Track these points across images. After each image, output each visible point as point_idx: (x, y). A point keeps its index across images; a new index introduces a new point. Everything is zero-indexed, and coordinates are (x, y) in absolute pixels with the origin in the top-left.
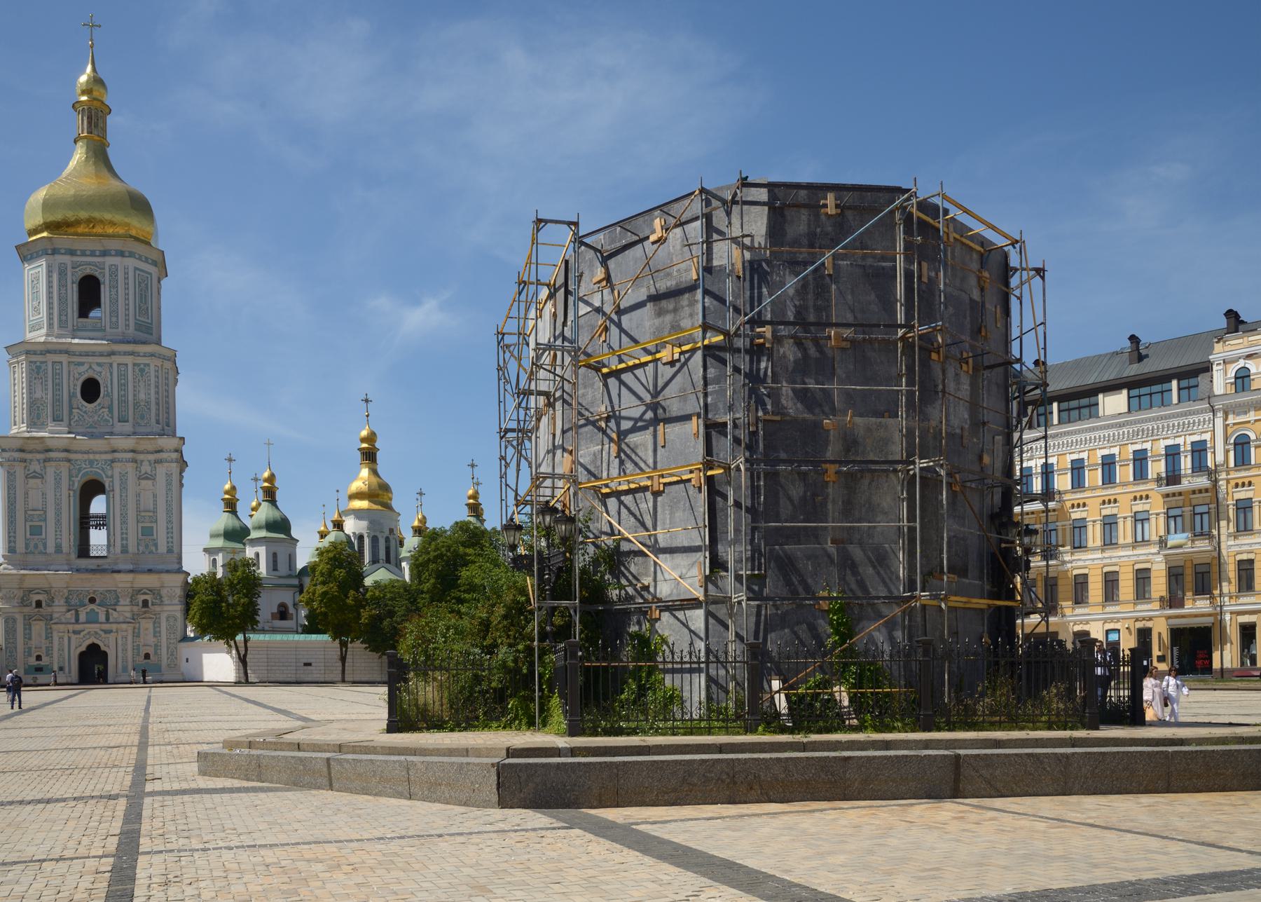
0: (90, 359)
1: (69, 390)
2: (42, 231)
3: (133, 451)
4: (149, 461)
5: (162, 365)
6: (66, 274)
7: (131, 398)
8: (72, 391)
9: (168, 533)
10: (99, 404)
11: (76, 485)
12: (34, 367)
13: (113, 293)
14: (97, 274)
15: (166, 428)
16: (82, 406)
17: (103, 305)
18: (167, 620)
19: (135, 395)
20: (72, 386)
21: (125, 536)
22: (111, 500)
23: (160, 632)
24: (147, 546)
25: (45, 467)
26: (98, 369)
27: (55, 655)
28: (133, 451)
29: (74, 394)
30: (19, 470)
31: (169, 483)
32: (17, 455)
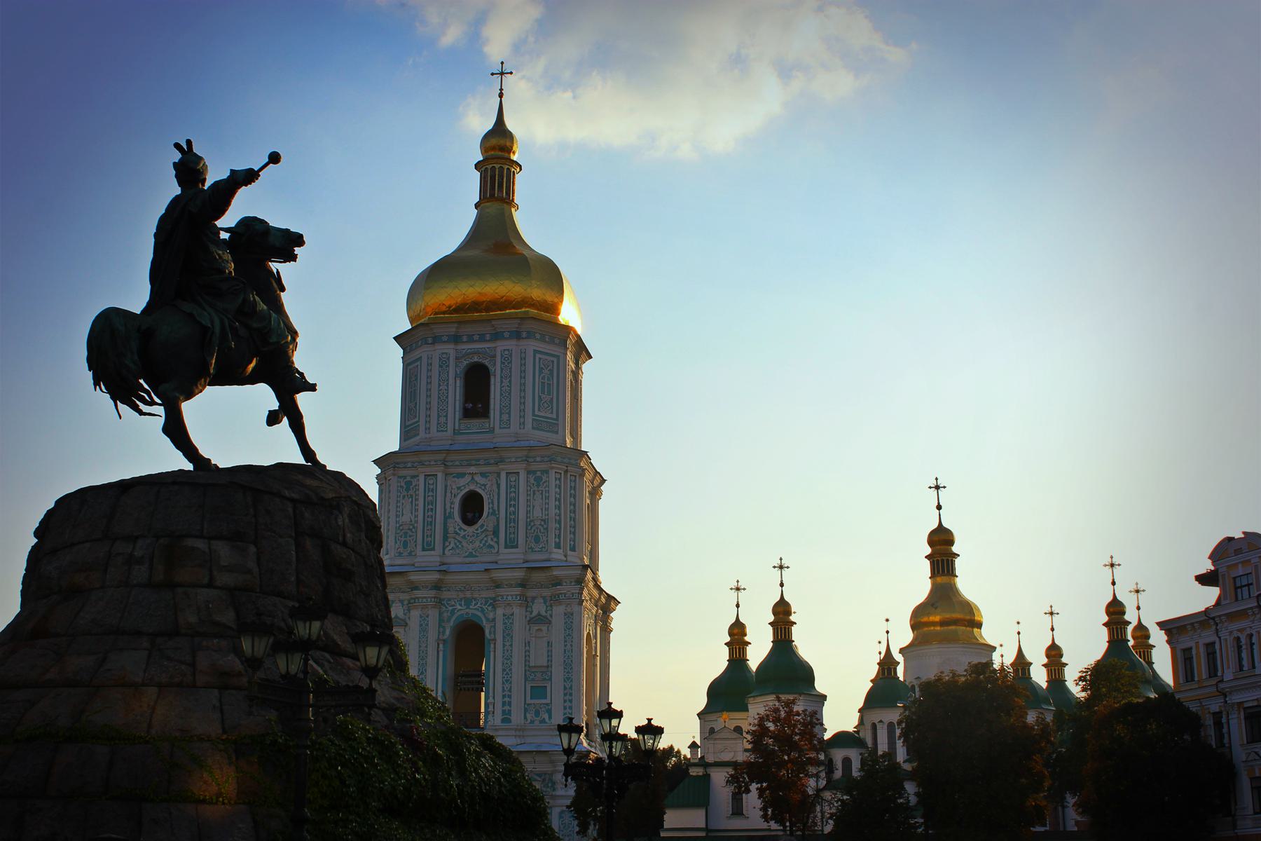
0: (473, 469)
1: (445, 510)
4: (544, 598)
6: (448, 366)
8: (448, 511)
9: (565, 695)
10: (482, 526)
11: (448, 632)
12: (403, 484)
13: (506, 382)
14: (486, 362)
15: (569, 552)
16: (460, 529)
21: (507, 699)
24: (537, 713)
25: (409, 610)
29: (451, 516)
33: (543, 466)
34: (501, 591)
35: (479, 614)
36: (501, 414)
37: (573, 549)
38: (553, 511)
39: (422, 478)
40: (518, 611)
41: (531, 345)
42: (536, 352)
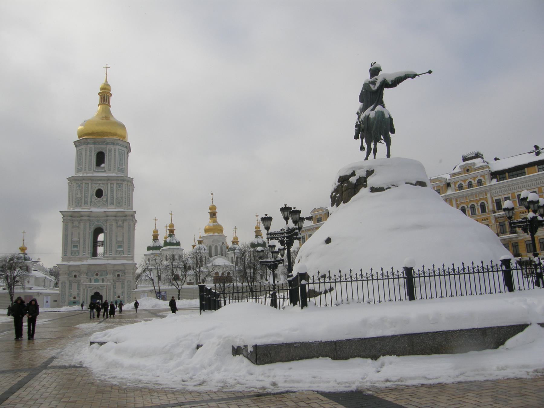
0: (100, 182)
2: (84, 136)
3: (115, 216)
4: (121, 220)
5: (128, 184)
7: (115, 196)
10: (103, 199)
13: (110, 157)
14: (104, 151)
17: (105, 163)
18: (127, 282)
19: (116, 195)
20: (92, 192)
21: (111, 249)
22: (106, 236)
23: (124, 287)
26: (102, 185)
27: (81, 297)
28: (115, 216)
30: (70, 225)
31: (129, 228)
32: (69, 218)
33: (121, 182)
34: (109, 218)
35: (101, 224)
36: (108, 166)
37: (129, 206)
38: (124, 195)
39: (84, 184)
40: (114, 224)
41: (118, 147)
42: (119, 149)
